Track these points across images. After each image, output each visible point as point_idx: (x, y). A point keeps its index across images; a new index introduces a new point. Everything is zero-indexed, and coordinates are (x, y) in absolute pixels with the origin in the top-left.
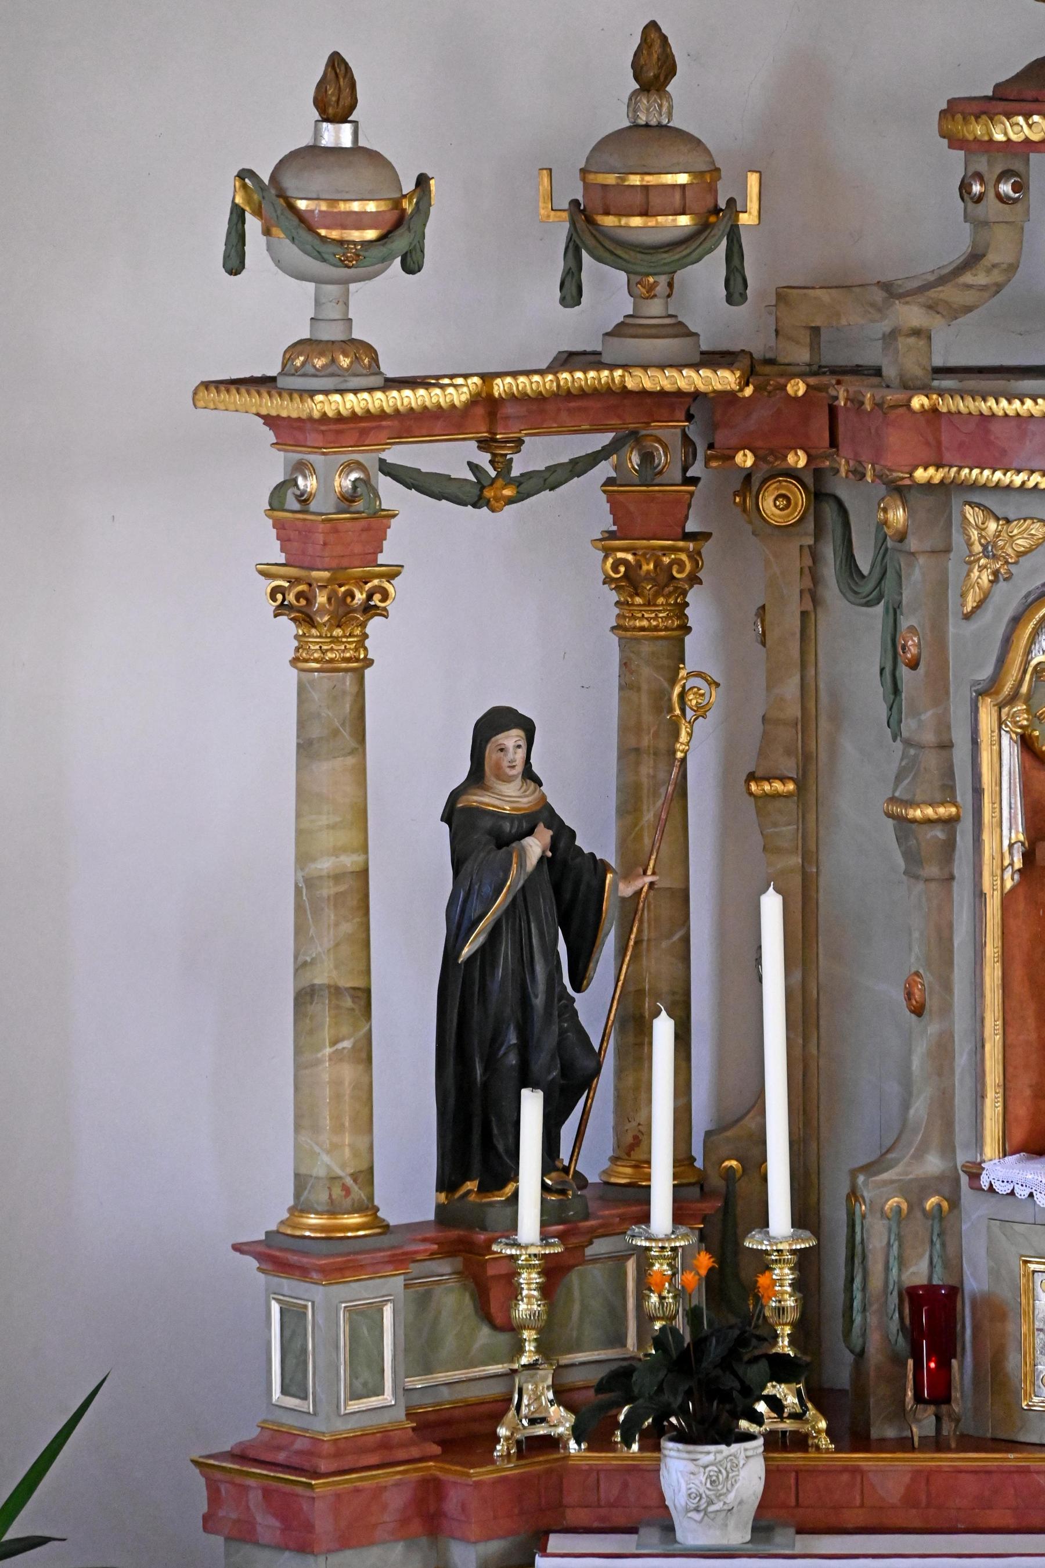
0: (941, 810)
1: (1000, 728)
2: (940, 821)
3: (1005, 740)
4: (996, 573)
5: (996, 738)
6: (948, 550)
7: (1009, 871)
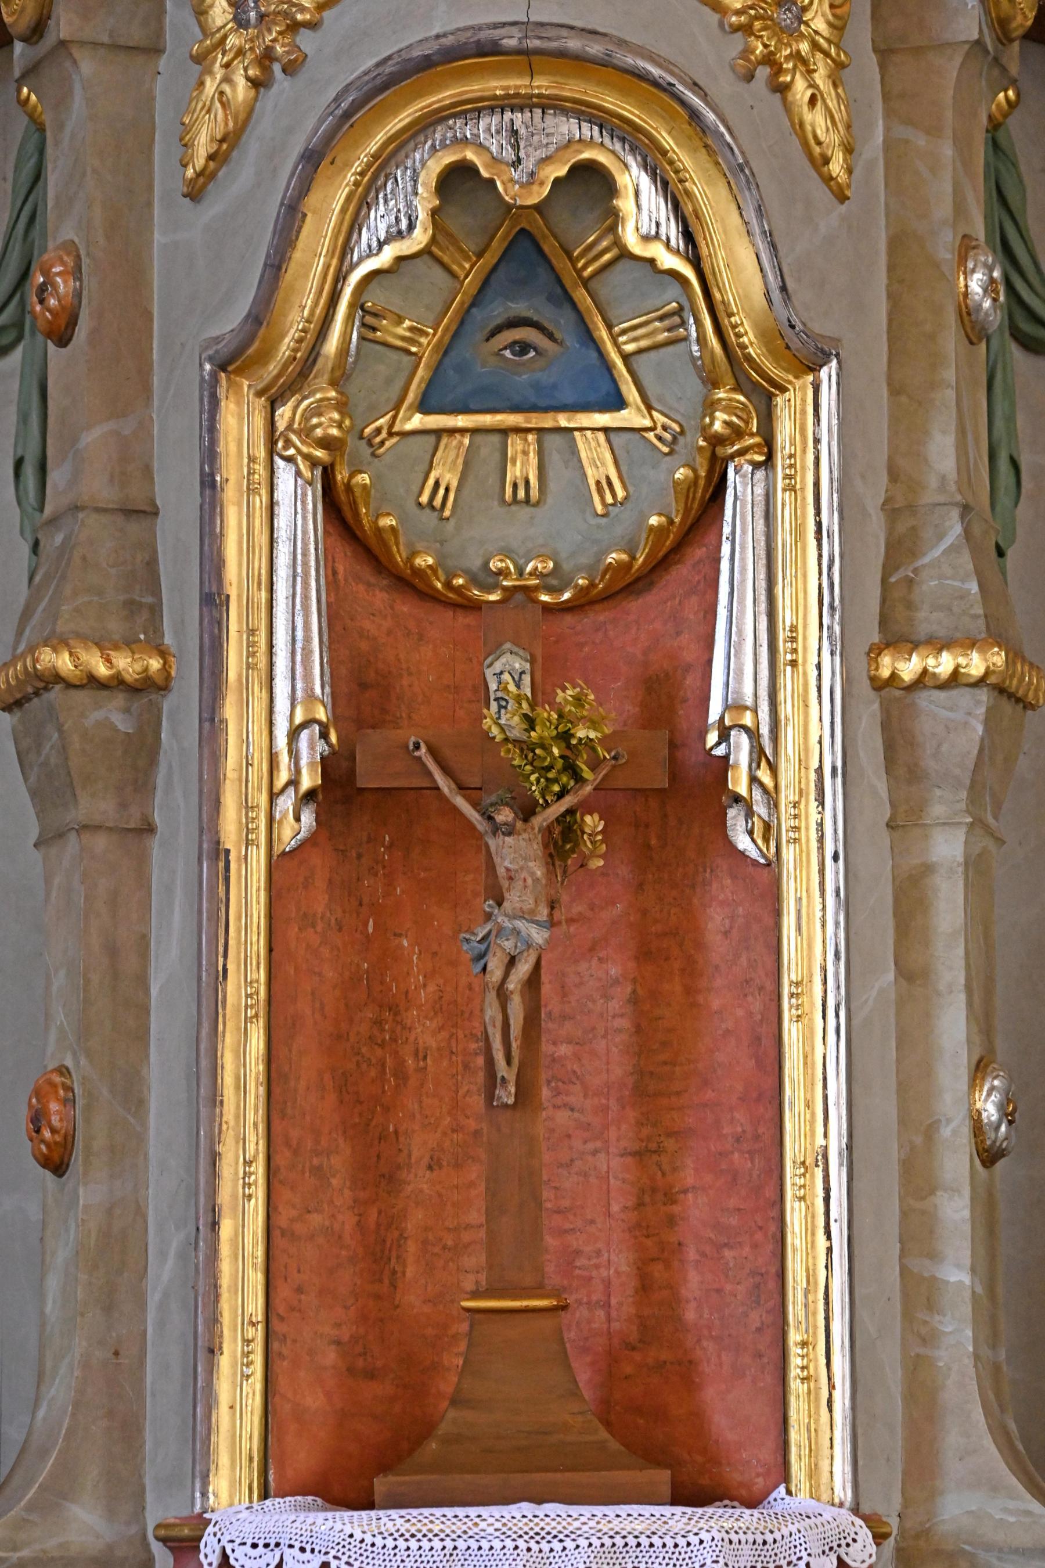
0: (125, 664)
1: (271, 452)
2: (117, 683)
3: (285, 475)
4: (267, 57)
5: (260, 469)
6: (155, 50)
7: (286, 803)
